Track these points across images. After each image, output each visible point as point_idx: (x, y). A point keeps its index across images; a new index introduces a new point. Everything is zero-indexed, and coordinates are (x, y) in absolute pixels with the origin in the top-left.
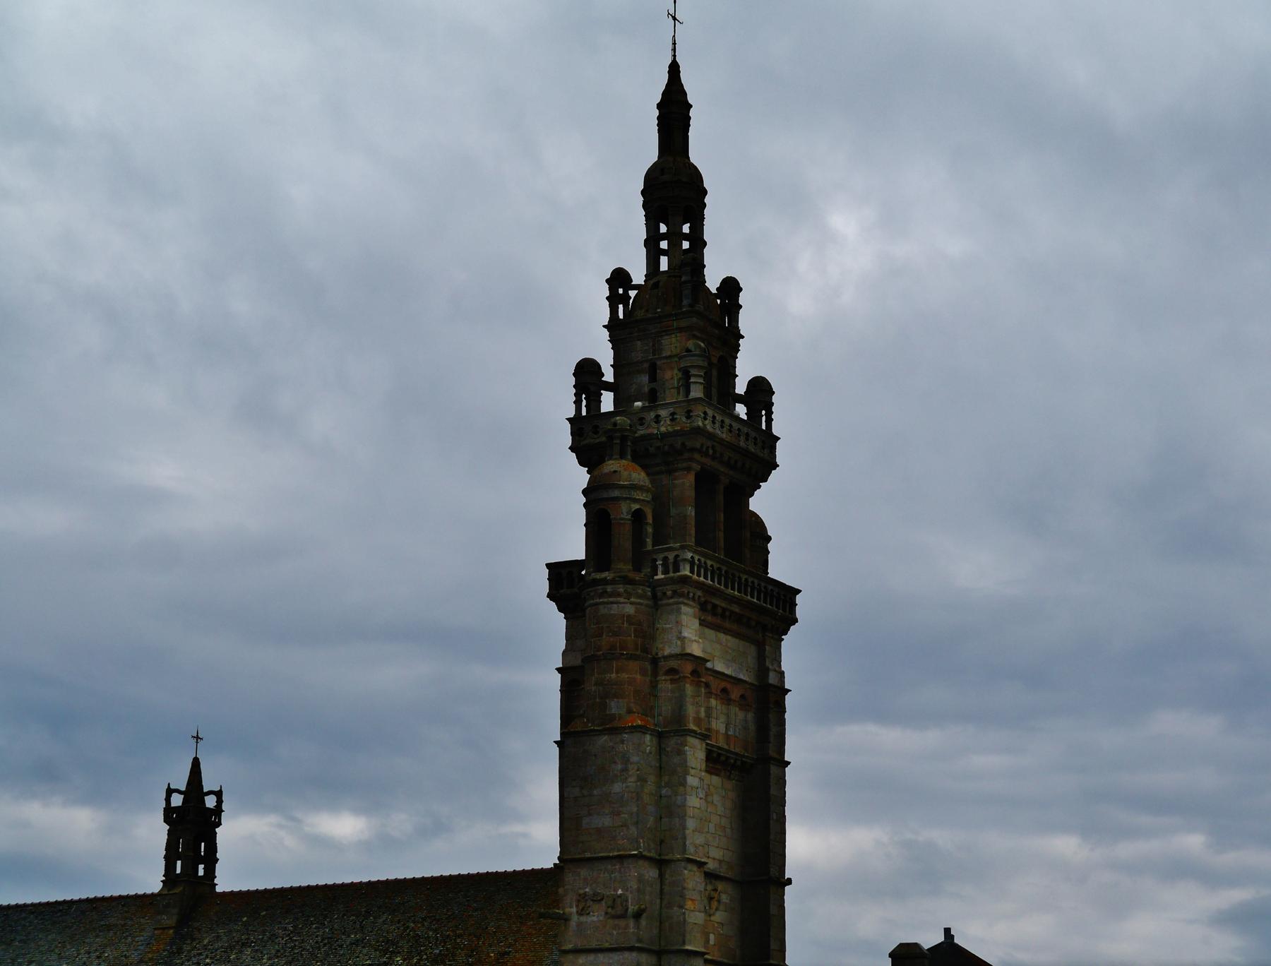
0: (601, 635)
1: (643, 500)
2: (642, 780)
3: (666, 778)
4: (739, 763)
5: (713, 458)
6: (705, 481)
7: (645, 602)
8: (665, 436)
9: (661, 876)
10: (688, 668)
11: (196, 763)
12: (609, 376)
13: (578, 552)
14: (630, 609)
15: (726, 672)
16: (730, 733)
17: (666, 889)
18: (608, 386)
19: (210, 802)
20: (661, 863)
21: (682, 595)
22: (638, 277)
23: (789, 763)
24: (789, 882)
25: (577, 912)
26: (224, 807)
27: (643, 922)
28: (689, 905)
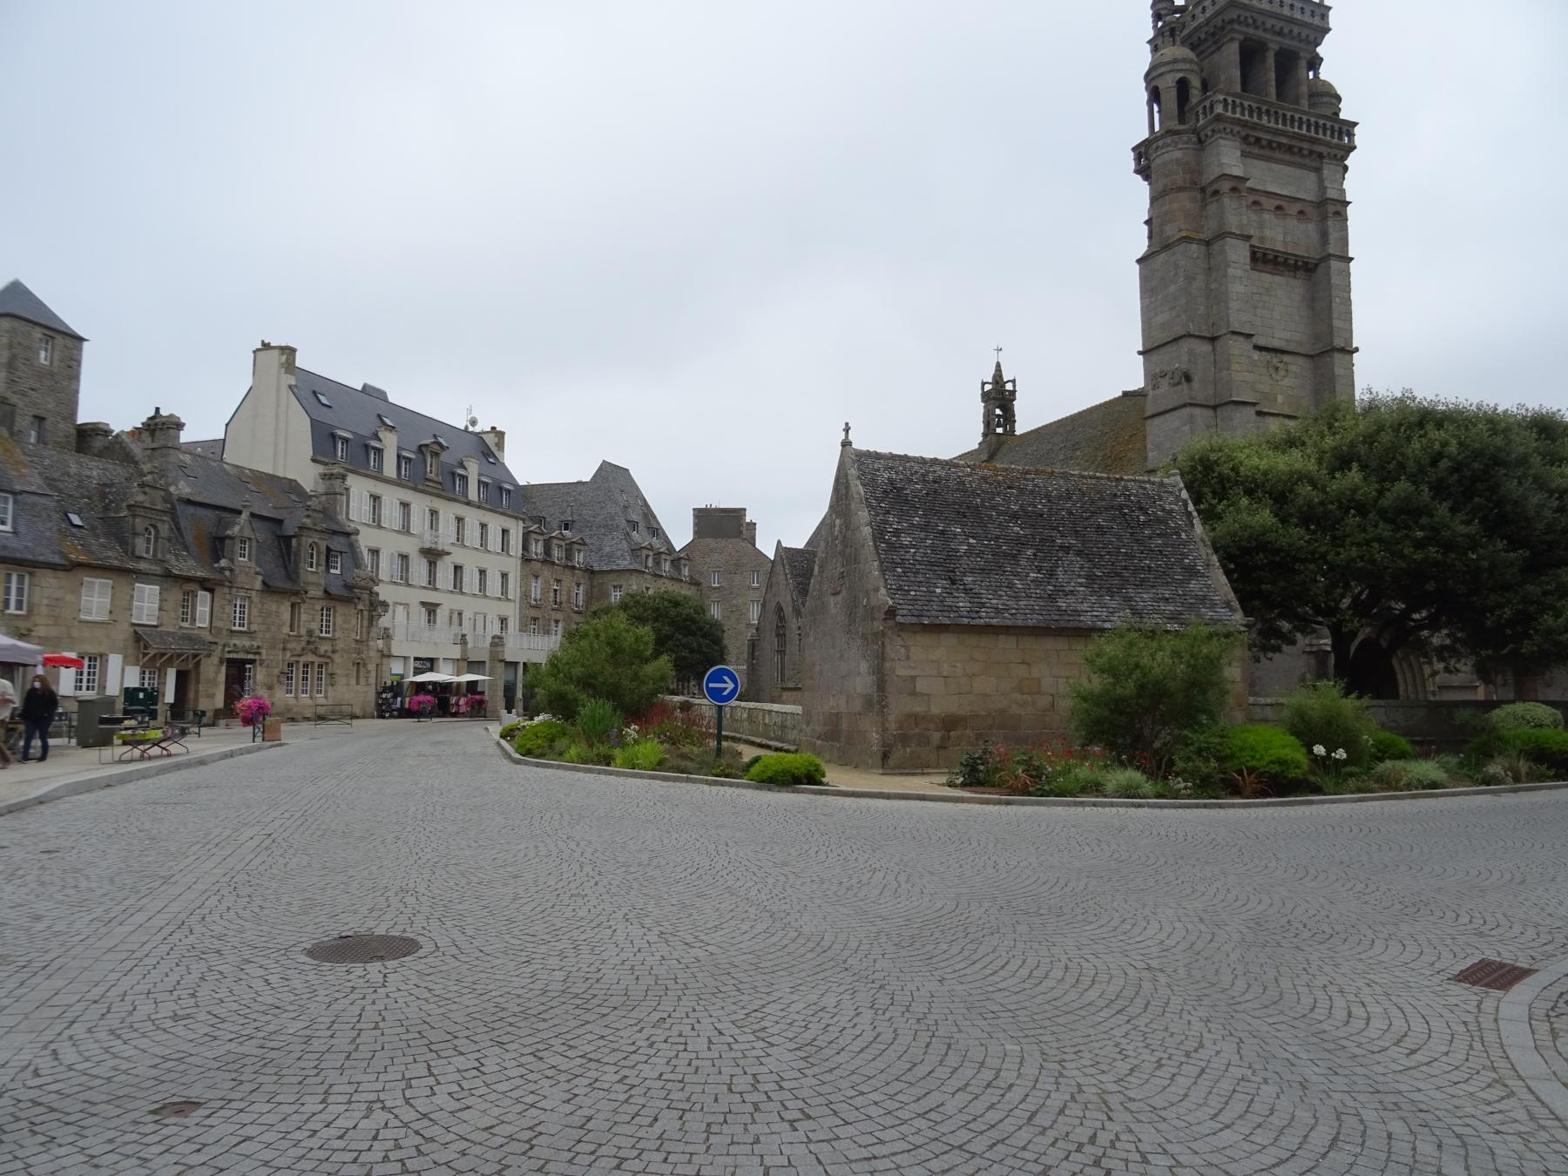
1: (1186, 70)
2: (1190, 279)
3: (1214, 275)
5: (1257, 28)
7: (1192, 146)
8: (1208, 21)
9: (1214, 349)
10: (1225, 186)
14: (1178, 154)
15: (1279, 192)
16: (1288, 239)
19: (1009, 387)
21: (1219, 131)
23: (1352, 259)
24: (1357, 350)
27: (1196, 384)
28: (1235, 367)
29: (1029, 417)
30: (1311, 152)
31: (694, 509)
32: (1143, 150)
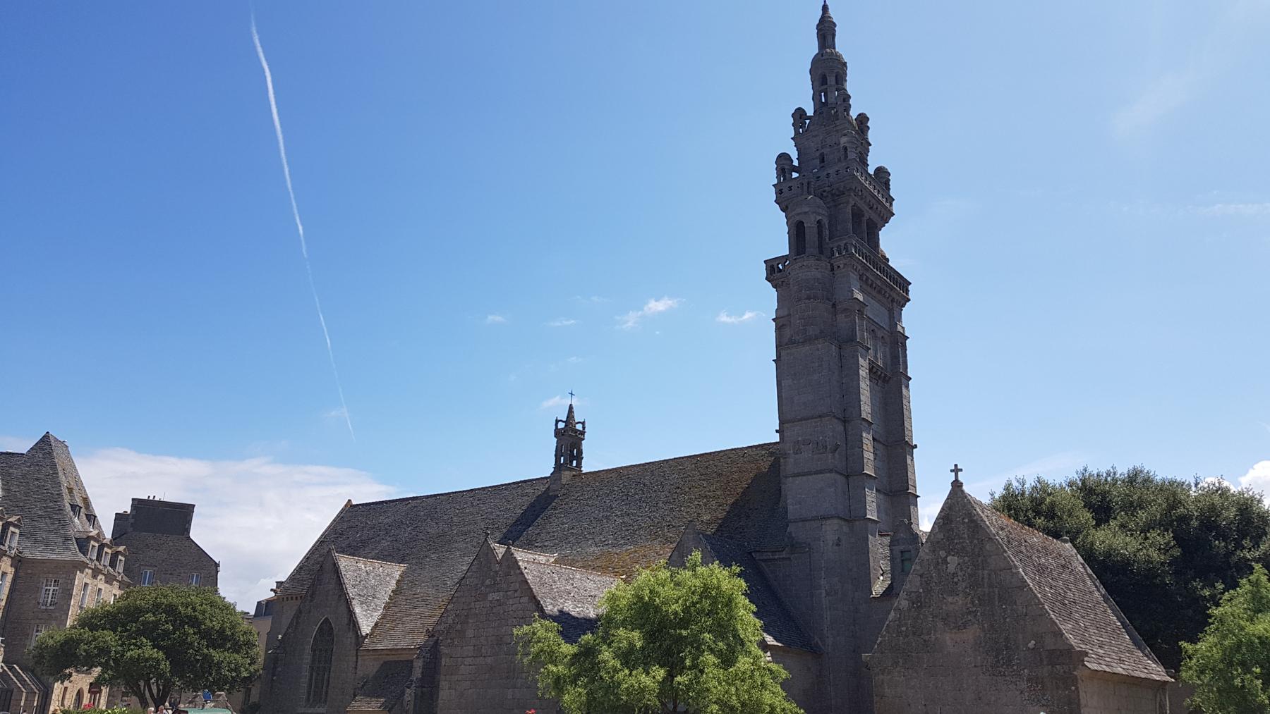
0: (801, 291)
4: (883, 375)
6: (857, 215)
11: (571, 407)
12: (796, 163)
13: (785, 251)
17: (849, 438)
18: (795, 169)
20: (845, 422)
22: (810, 112)
24: (916, 446)
25: (794, 452)
26: (586, 430)
29: (594, 459)
30: (890, 296)
31: (133, 499)
32: (775, 264)
